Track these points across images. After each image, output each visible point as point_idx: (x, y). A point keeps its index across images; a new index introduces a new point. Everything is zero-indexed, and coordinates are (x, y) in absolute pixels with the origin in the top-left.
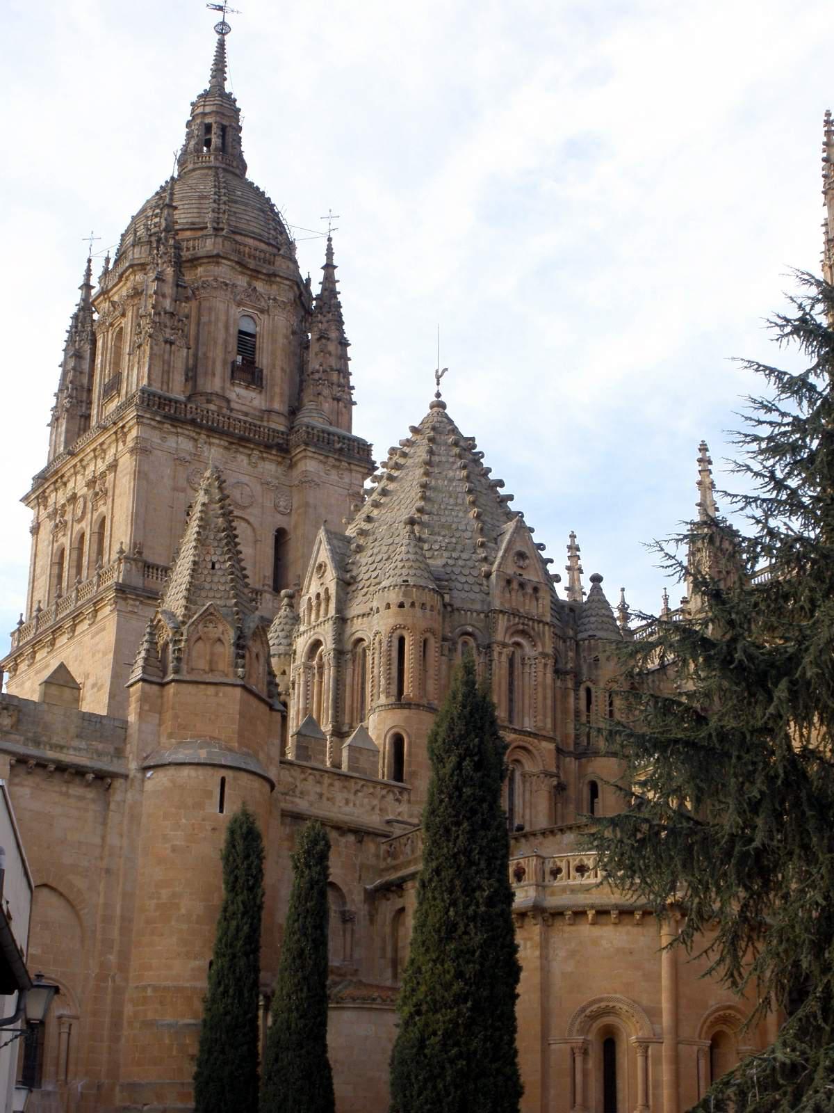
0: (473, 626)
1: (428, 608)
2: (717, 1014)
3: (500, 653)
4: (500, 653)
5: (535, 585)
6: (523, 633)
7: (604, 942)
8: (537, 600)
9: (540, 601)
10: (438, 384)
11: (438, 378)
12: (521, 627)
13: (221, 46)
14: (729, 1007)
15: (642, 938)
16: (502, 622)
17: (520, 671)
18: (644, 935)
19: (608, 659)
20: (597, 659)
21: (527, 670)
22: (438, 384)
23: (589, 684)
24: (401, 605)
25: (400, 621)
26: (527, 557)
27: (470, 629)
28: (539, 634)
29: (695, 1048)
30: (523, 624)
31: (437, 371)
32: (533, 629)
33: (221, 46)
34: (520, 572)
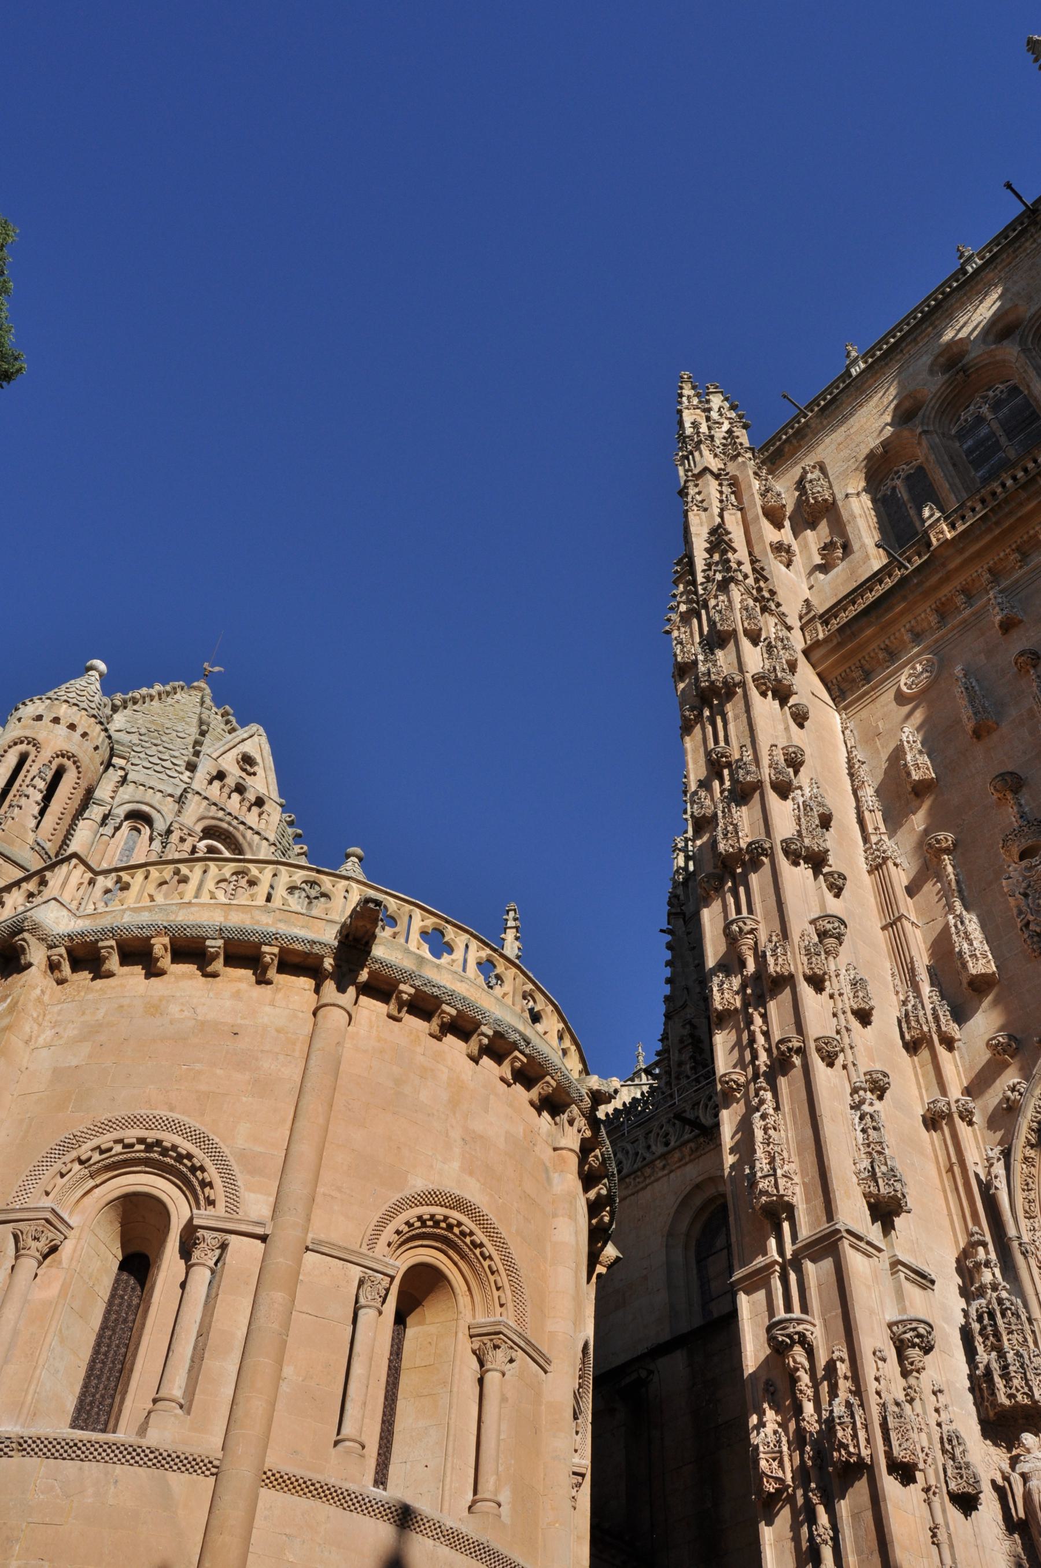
1: (80, 731)
2: (426, 1211)
3: (182, 840)
4: (182, 840)
5: (261, 795)
7: (174, 1009)
8: (260, 815)
9: (264, 816)
12: (225, 825)
14: (459, 1204)
15: (268, 1009)
16: (194, 808)
18: (272, 1004)
24: (39, 718)
25: (28, 733)
27: (146, 808)
28: (250, 845)
29: (356, 1272)
30: (229, 824)
32: (244, 837)
34: (244, 775)
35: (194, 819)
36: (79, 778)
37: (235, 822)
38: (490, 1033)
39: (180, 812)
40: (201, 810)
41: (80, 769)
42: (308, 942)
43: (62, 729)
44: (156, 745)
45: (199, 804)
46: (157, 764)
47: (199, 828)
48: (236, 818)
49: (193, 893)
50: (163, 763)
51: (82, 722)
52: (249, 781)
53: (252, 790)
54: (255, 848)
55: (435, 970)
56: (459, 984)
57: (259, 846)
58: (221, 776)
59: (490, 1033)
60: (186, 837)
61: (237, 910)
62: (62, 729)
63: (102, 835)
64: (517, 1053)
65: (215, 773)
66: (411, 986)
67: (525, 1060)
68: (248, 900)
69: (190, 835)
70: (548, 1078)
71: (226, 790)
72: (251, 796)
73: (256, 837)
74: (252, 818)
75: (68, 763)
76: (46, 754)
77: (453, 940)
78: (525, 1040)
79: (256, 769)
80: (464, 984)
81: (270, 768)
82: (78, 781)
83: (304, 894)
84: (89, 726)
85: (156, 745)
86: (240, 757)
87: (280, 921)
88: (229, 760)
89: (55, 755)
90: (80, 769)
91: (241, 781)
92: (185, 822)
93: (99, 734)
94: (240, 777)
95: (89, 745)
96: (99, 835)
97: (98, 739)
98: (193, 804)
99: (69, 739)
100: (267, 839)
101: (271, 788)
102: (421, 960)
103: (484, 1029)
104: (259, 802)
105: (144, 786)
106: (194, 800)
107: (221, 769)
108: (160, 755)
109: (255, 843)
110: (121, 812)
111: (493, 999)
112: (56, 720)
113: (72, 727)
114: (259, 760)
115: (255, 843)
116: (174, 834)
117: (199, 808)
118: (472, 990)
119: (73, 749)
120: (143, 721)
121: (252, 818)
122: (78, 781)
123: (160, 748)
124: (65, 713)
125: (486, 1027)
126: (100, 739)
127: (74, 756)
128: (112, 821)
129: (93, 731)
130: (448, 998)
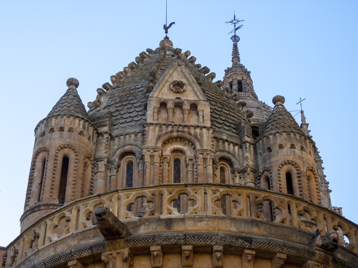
0: (131, 145)
1: (66, 129)
4: (152, 156)
5: (193, 102)
6: (180, 139)
9: (201, 113)
10: (166, 32)
11: (166, 28)
12: (175, 134)
13: (235, 47)
17: (185, 173)
19: (281, 147)
20: (270, 150)
21: (190, 169)
22: (166, 32)
23: (266, 173)
26: (184, 84)
28: (196, 137)
31: (165, 26)
32: (190, 134)
33: (235, 47)
35: (154, 141)
36: (76, 156)
37: (181, 129)
38: (221, 248)
39: (144, 141)
40: (157, 133)
41: (76, 150)
42: (89, 249)
43: (56, 134)
44: (126, 105)
45: (154, 130)
46: (128, 118)
47: (160, 145)
48: (180, 125)
49: (42, 242)
50: (132, 115)
51: (66, 123)
52: (183, 97)
53: (186, 102)
54: (199, 137)
55: (181, 223)
56: (199, 224)
57: (201, 135)
58: (163, 104)
59: (221, 248)
60: (153, 154)
61: (60, 244)
62: (56, 134)
63: (110, 177)
64: (246, 251)
65: (159, 106)
66: (157, 245)
67: (254, 253)
68: (67, 233)
69: (155, 151)
70: (278, 255)
71: (171, 112)
72: (187, 107)
73: (198, 130)
74: (193, 120)
75: (66, 151)
76: (53, 152)
77: (193, 196)
78: (247, 241)
79: (185, 87)
80: (203, 223)
81: (194, 82)
82: (77, 157)
83: (248, 144)
84: (71, 123)
85: (126, 105)
86: (172, 86)
87: (81, 240)
88: (166, 92)
89: (59, 148)
90: (76, 150)
91: (177, 101)
92: (149, 145)
93: (79, 124)
94: (177, 98)
95: (75, 134)
96: (108, 178)
97: (79, 127)
98: (151, 132)
99: (61, 137)
100: (205, 127)
101: (199, 94)
102: (169, 222)
103: (215, 248)
104: (194, 106)
105: (123, 135)
106: (151, 130)
107: (162, 101)
108: (129, 111)
109: (198, 134)
110: (116, 158)
111: (228, 221)
112: (52, 130)
113: (62, 129)
114: (184, 81)
115: (198, 134)
116: (146, 156)
117: (155, 133)
118: (209, 223)
119: (68, 141)
120: (119, 93)
121: (193, 120)
122: (77, 157)
123: (129, 106)
124: (55, 123)
125: (216, 246)
126: (81, 126)
127: (68, 145)
128: (113, 166)
129: (74, 124)
130: (183, 241)
